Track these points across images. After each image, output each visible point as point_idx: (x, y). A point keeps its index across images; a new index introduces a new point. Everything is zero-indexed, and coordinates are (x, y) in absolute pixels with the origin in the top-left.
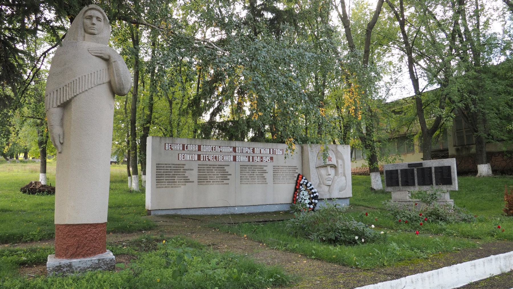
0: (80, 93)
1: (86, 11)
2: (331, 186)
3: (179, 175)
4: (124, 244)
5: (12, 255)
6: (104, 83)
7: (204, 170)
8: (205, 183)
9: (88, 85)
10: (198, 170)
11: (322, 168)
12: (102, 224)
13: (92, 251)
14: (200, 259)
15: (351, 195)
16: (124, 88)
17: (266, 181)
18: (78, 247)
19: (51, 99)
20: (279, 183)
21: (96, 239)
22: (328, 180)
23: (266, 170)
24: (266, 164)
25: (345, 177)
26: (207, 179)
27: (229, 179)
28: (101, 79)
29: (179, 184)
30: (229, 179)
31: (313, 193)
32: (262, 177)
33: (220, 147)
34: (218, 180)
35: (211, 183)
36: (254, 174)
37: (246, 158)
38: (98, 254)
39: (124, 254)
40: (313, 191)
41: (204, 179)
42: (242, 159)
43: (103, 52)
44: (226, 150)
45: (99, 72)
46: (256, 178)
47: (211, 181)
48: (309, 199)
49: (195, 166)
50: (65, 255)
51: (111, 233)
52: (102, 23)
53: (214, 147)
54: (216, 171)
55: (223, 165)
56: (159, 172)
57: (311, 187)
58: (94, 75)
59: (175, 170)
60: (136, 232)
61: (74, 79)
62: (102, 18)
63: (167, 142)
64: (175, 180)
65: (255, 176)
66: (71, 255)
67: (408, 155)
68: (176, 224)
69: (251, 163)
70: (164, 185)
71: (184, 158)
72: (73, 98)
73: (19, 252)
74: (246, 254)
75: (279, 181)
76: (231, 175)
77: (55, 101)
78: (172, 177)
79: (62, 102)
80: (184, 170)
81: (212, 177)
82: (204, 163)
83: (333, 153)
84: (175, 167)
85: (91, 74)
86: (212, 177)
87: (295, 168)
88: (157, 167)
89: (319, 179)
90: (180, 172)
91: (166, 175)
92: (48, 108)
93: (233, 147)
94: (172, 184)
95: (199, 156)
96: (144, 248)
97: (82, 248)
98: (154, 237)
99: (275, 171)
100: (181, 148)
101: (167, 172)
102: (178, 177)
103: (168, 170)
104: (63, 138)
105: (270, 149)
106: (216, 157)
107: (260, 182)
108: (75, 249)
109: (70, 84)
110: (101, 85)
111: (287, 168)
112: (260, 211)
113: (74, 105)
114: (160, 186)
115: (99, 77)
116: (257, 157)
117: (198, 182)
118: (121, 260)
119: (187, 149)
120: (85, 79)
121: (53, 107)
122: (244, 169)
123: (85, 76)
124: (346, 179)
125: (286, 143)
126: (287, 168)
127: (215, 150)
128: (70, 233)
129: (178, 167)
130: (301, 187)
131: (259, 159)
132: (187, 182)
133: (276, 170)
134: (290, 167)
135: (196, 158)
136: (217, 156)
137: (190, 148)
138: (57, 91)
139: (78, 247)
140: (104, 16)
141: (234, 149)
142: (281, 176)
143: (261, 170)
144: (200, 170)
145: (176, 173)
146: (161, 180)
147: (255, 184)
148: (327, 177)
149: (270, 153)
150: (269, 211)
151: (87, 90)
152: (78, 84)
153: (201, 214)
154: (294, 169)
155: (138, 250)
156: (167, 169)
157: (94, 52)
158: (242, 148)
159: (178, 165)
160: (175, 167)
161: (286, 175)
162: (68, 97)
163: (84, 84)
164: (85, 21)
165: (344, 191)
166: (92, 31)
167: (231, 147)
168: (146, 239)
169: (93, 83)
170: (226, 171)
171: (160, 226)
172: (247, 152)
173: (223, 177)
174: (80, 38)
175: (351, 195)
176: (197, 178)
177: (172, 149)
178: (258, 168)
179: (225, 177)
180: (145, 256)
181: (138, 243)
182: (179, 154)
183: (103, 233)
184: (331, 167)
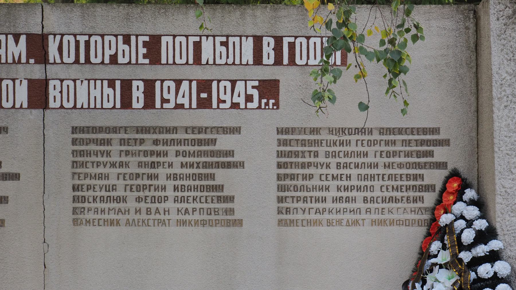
17: (231, 211)
20: (317, 223)
23: (230, 153)
32: (202, 188)
36: (160, 171)
46: (170, 193)
57: (481, 250)
65: (161, 182)
75: (317, 212)
76: (16, 177)
93: (30, 37)
99: (289, 154)
105: (258, 41)
107: (197, 216)
116: (178, 83)
122: (93, 147)
126: (376, 136)
134: (391, 131)
143: (200, 154)
147: (162, 223)
149: (258, 59)
154: (422, 143)
158: (82, 39)
161: (366, 178)
167: (17, 38)
172: (114, 59)
178: (179, 142)
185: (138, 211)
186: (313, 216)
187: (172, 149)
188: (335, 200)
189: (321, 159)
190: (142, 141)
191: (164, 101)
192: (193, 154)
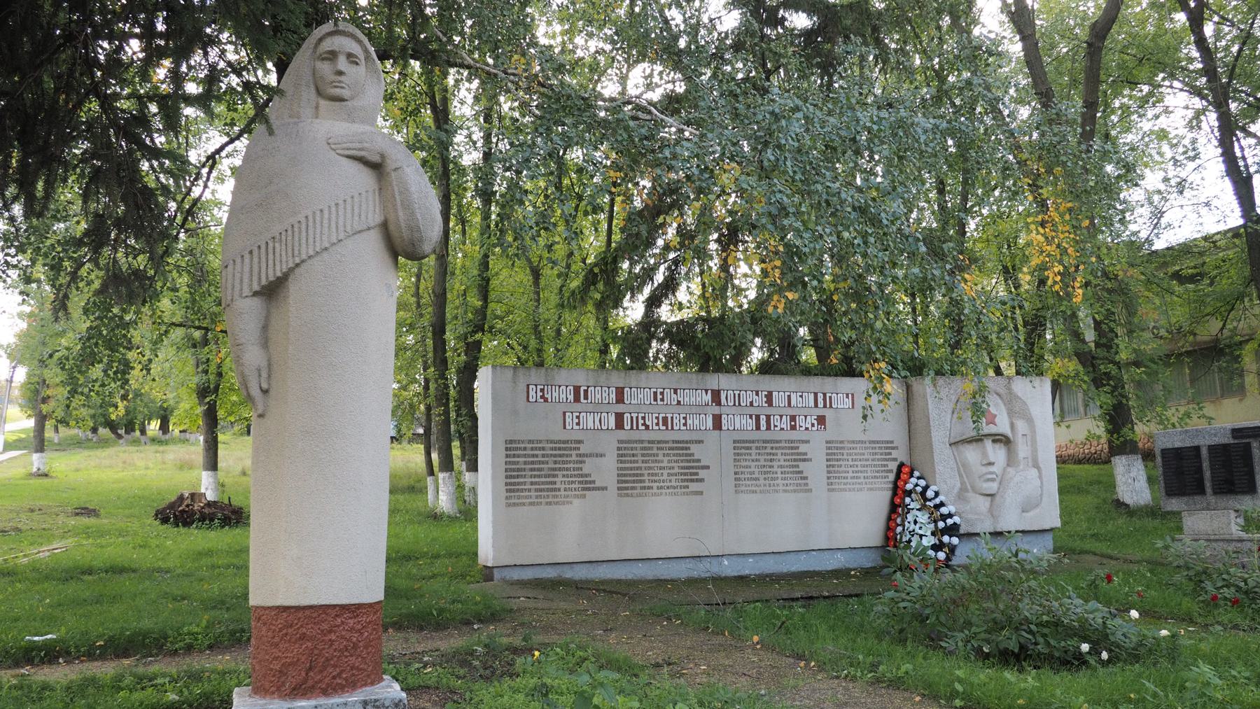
0: (310, 257)
1: (321, 40)
2: (998, 498)
3: (567, 469)
4: (425, 659)
5: (143, 689)
6: (369, 229)
7: (633, 455)
8: (638, 491)
9: (329, 236)
10: (619, 455)
11: (967, 446)
12: (371, 605)
13: (346, 679)
14: (637, 704)
15: (1057, 523)
16: (421, 240)
17: (806, 484)
18: (310, 669)
19: (238, 275)
21: (355, 646)
22: (989, 480)
23: (805, 454)
24: (804, 436)
25: (1038, 468)
26: (643, 481)
27: (702, 480)
28: (363, 217)
29: (568, 496)
30: (702, 480)
31: (944, 517)
32: (793, 473)
33: (675, 392)
34: (673, 484)
35: (655, 490)
36: (775, 464)
37: (749, 421)
38: (361, 687)
39: (428, 688)
40: (944, 510)
41: (634, 482)
42: (738, 422)
43: (366, 145)
44: (693, 399)
45: (356, 200)
46: (779, 475)
47: (655, 485)
48: (933, 534)
49: (609, 444)
50: (278, 689)
51: (390, 630)
52: (362, 69)
53: (659, 390)
54: (666, 459)
55: (687, 442)
56: (514, 463)
57: (937, 501)
58: (345, 209)
59: (555, 456)
60: (456, 628)
61: (293, 220)
62: (362, 56)
63: (534, 379)
64: (555, 483)
65: (775, 469)
66: (294, 689)
67: (1226, 402)
68: (563, 605)
69: (764, 434)
70: (526, 497)
71: (578, 424)
72: (291, 270)
73: (159, 681)
74: (763, 692)
76: (708, 467)
77: (246, 280)
78: (549, 476)
79: (264, 282)
80: (580, 455)
81: (656, 475)
82: (635, 435)
83: (1000, 401)
84: (555, 449)
85: (337, 205)
86: (656, 475)
87: (889, 446)
88: (507, 449)
89: (960, 475)
90: (570, 462)
91: (532, 470)
92: (229, 298)
94: (548, 496)
95: (619, 418)
96: (482, 671)
97: (321, 672)
98: (505, 640)
100: (571, 397)
101: (533, 463)
102: (564, 476)
103: (537, 456)
104: (269, 376)
105: (816, 395)
106: (665, 420)
107: (791, 488)
108: (303, 674)
109: (284, 233)
110: (365, 235)
111: (868, 445)
112: (794, 569)
113: (294, 289)
114: (517, 501)
115: (356, 211)
117: (619, 489)
118: (422, 703)
119: (586, 398)
120: (322, 219)
121: (241, 296)
122: (743, 451)
123: (321, 211)
124: (1040, 477)
125: (866, 375)
126: (868, 445)
127: (662, 400)
128: (290, 630)
129: (565, 449)
130: (908, 500)
131: (785, 423)
132: (588, 489)
133: (834, 451)
134: (874, 442)
135: (612, 424)
136: (669, 416)
137: (596, 395)
138: (251, 252)
139: (310, 669)
140: (366, 51)
141: (716, 396)
142: (850, 469)
143: (792, 454)
144: (622, 455)
145: (557, 466)
146: (519, 484)
147: (777, 491)
148: (985, 470)
150: (817, 569)
151: (326, 249)
152: (304, 234)
153: (630, 577)
154: (887, 448)
155: (465, 677)
156: (533, 456)
157: (345, 145)
158: (737, 393)
159: (567, 442)
160: (555, 449)
162: (278, 268)
163: (318, 231)
164: (319, 65)
165: (1037, 511)
166: (337, 92)
168: (485, 646)
169: (341, 229)
170: (696, 457)
171: (519, 610)
173: (685, 474)
174: (307, 112)
175: (1057, 523)
176: (616, 478)
177: (546, 400)
178: (783, 448)
179: (692, 474)
180: (485, 692)
181: (463, 658)
182: (564, 413)
183: (374, 629)
184: (994, 441)
185: (765, 485)
186: (842, 487)
187: (779, 452)
188: (853, 478)
189: (845, 457)
190: (766, 448)
191: (775, 426)
192: (788, 454)
